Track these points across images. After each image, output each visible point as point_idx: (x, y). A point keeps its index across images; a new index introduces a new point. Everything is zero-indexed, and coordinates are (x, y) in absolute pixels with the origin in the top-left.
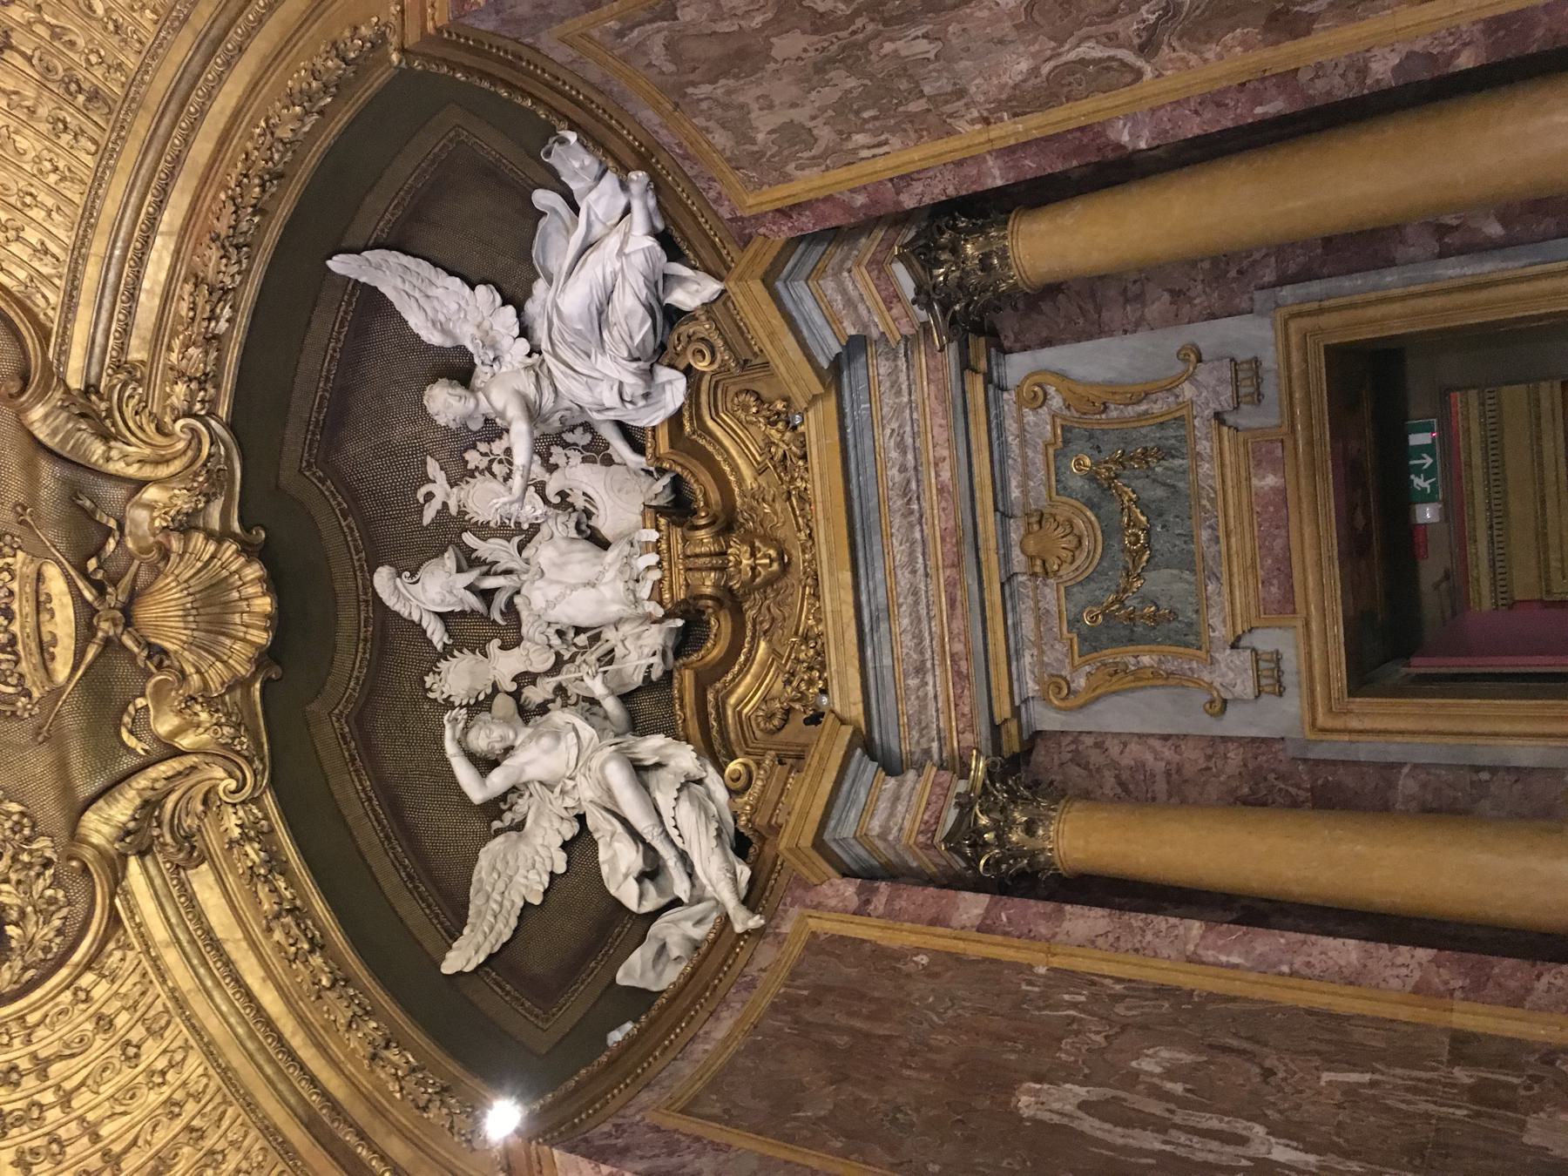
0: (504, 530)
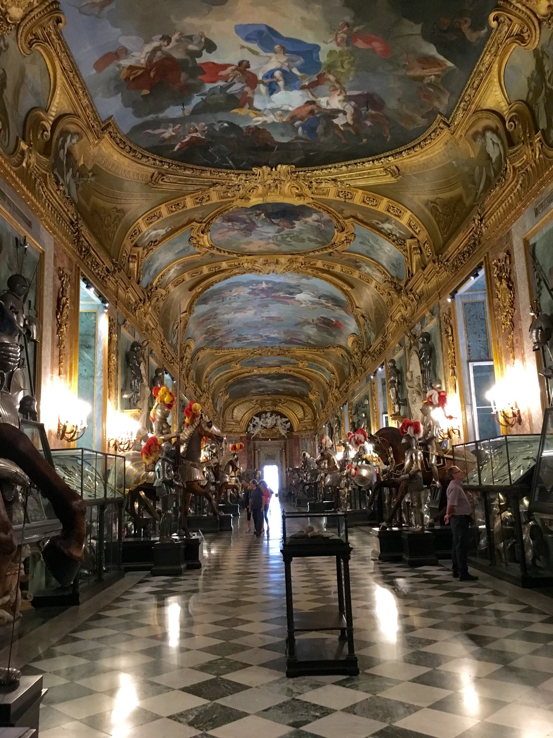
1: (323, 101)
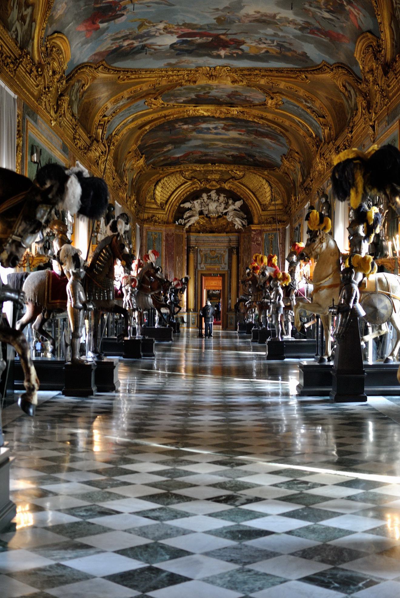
0: (219, 199)
1: (191, 126)
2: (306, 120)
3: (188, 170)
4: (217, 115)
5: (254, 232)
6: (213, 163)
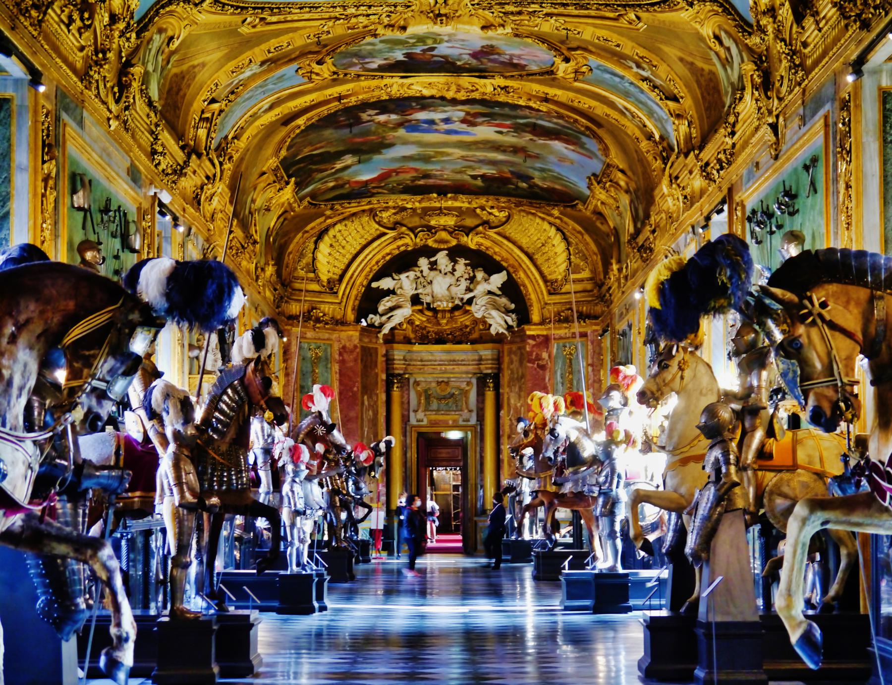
0: (454, 270)
1: (394, 117)
2: (639, 103)
3: (386, 209)
4: (450, 95)
5: (531, 342)
6: (442, 191)
